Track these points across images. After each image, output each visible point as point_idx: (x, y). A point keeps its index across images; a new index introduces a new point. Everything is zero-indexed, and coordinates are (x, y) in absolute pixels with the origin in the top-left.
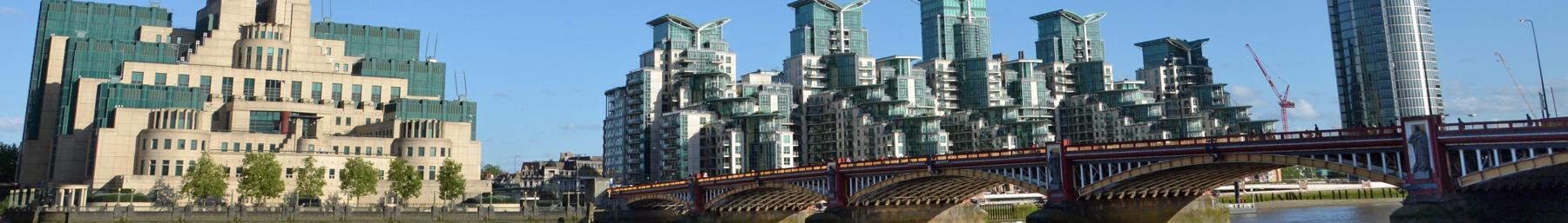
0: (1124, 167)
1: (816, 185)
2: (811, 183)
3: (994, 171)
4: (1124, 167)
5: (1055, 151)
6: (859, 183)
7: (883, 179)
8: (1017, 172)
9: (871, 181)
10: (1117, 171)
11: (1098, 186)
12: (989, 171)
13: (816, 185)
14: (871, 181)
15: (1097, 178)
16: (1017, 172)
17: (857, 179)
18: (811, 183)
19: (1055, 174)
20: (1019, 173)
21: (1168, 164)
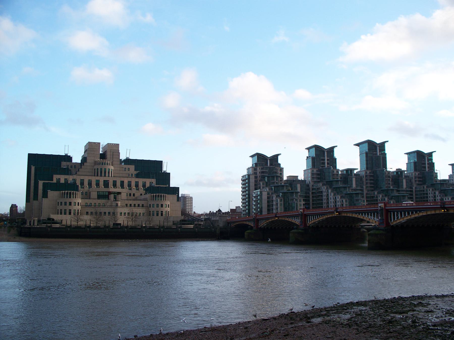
0: (409, 214)
1: (296, 218)
2: (295, 218)
3: (359, 214)
4: (409, 214)
5: (382, 206)
6: (311, 218)
7: (320, 216)
8: (368, 215)
9: (315, 217)
10: (406, 215)
11: (398, 221)
12: (358, 214)
13: (296, 218)
14: (315, 217)
15: (398, 218)
16: (368, 215)
17: (310, 216)
18: (295, 218)
19: (382, 216)
20: (369, 215)
21: (426, 213)
